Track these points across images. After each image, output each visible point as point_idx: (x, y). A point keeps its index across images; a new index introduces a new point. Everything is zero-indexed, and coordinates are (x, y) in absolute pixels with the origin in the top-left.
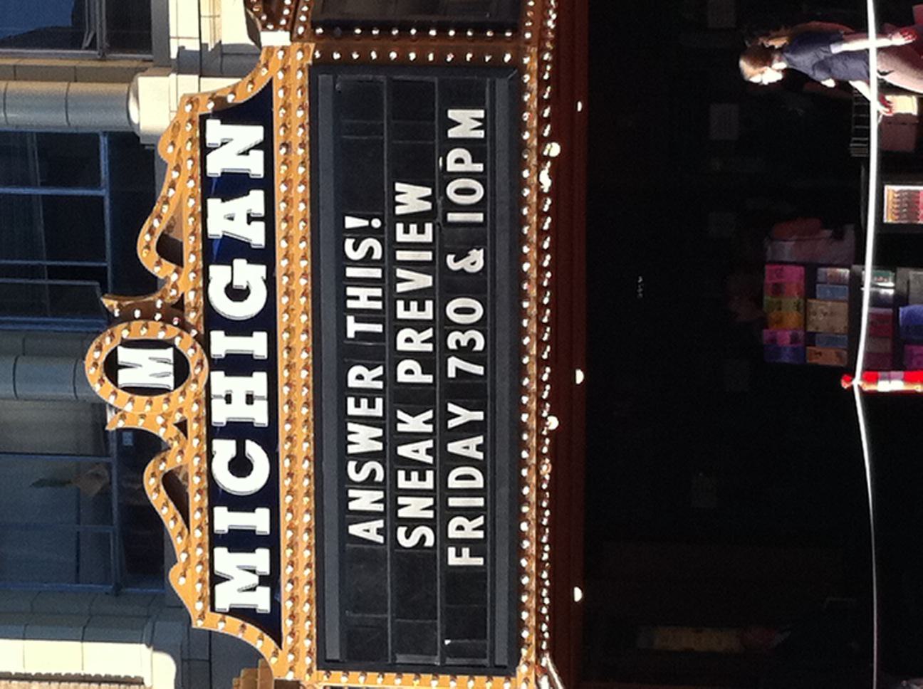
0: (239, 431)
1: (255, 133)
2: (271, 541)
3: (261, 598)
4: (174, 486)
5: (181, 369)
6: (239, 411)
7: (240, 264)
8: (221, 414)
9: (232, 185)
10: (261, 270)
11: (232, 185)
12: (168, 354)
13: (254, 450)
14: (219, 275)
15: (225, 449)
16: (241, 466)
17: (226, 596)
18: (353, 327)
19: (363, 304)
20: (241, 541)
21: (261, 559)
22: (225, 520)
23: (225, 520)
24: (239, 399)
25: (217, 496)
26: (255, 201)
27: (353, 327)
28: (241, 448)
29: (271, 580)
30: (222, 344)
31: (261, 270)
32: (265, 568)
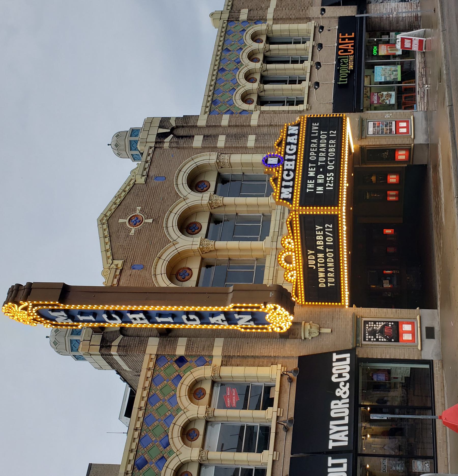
0: (288, 170)
1: (297, 128)
2: (293, 187)
3: (290, 196)
4: (275, 180)
5: (279, 161)
6: (289, 167)
7: (292, 145)
8: (286, 167)
9: (292, 135)
10: (296, 146)
11: (292, 135)
12: (277, 159)
13: (291, 173)
14: (288, 147)
15: (286, 173)
16: (288, 175)
17: (283, 196)
18: (308, 190)
19: (310, 187)
20: (286, 187)
21: (290, 190)
22: (284, 183)
23: (284, 183)
24: (289, 165)
25: (283, 179)
26: (296, 137)
27: (308, 190)
28: (289, 172)
29: (292, 193)
30: (287, 157)
31: (296, 146)
32: (291, 191)
